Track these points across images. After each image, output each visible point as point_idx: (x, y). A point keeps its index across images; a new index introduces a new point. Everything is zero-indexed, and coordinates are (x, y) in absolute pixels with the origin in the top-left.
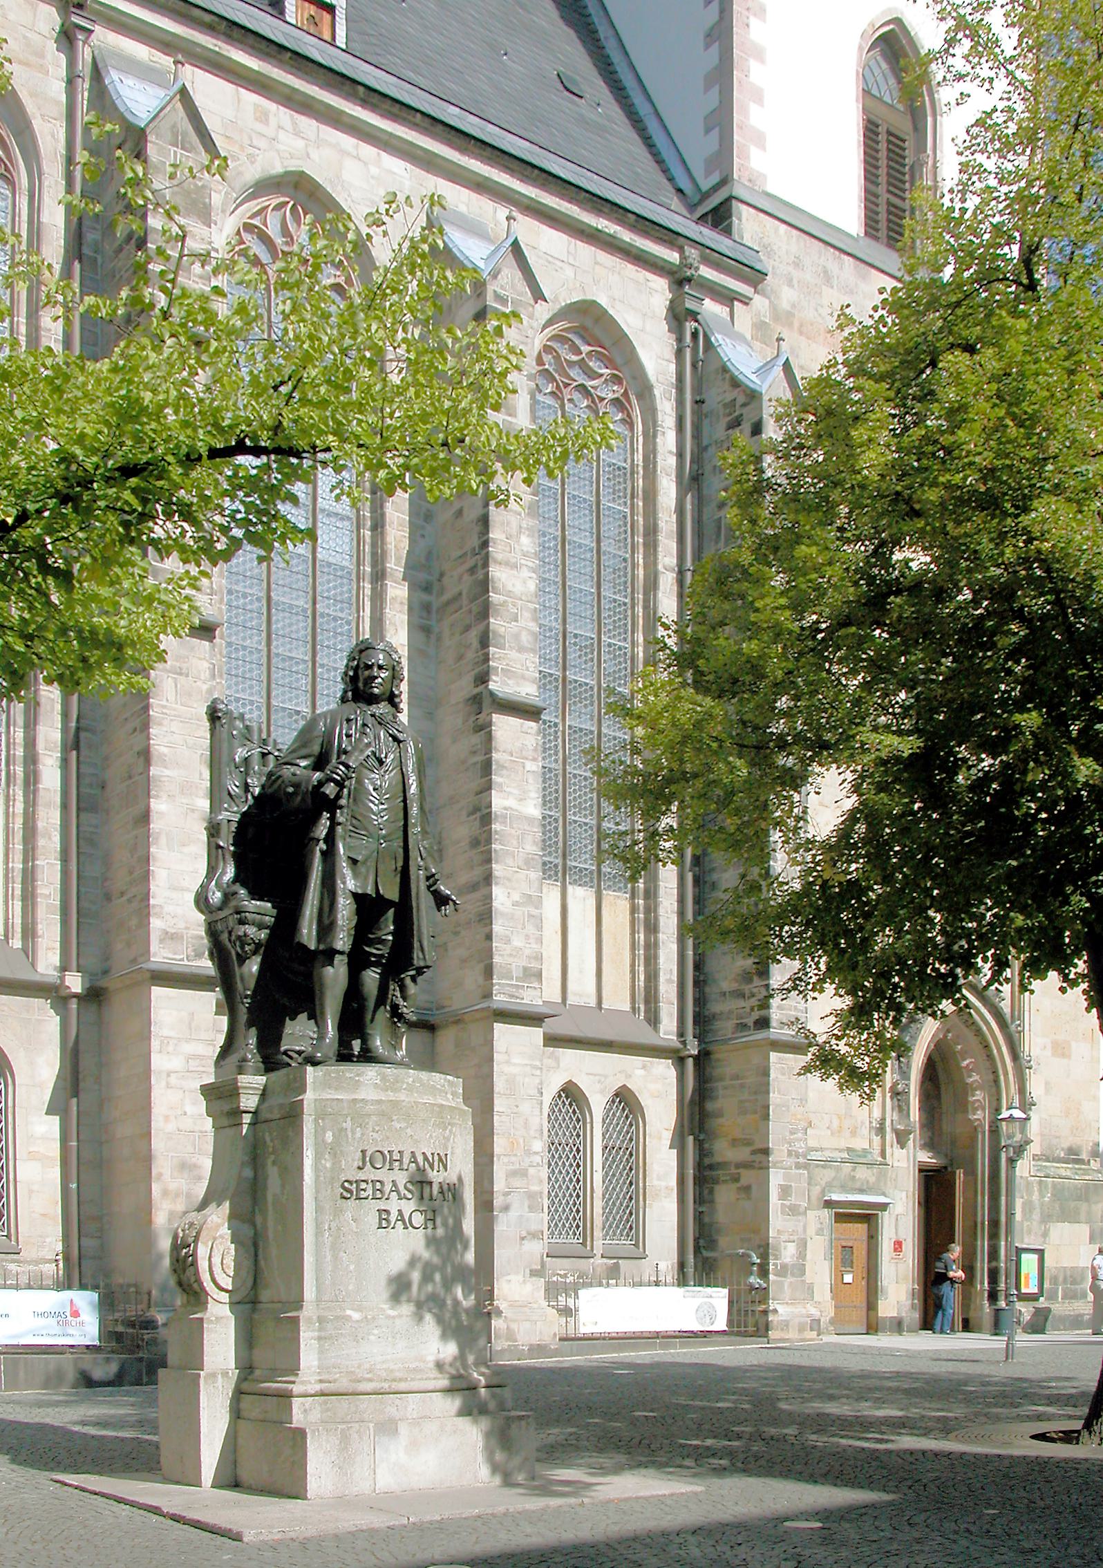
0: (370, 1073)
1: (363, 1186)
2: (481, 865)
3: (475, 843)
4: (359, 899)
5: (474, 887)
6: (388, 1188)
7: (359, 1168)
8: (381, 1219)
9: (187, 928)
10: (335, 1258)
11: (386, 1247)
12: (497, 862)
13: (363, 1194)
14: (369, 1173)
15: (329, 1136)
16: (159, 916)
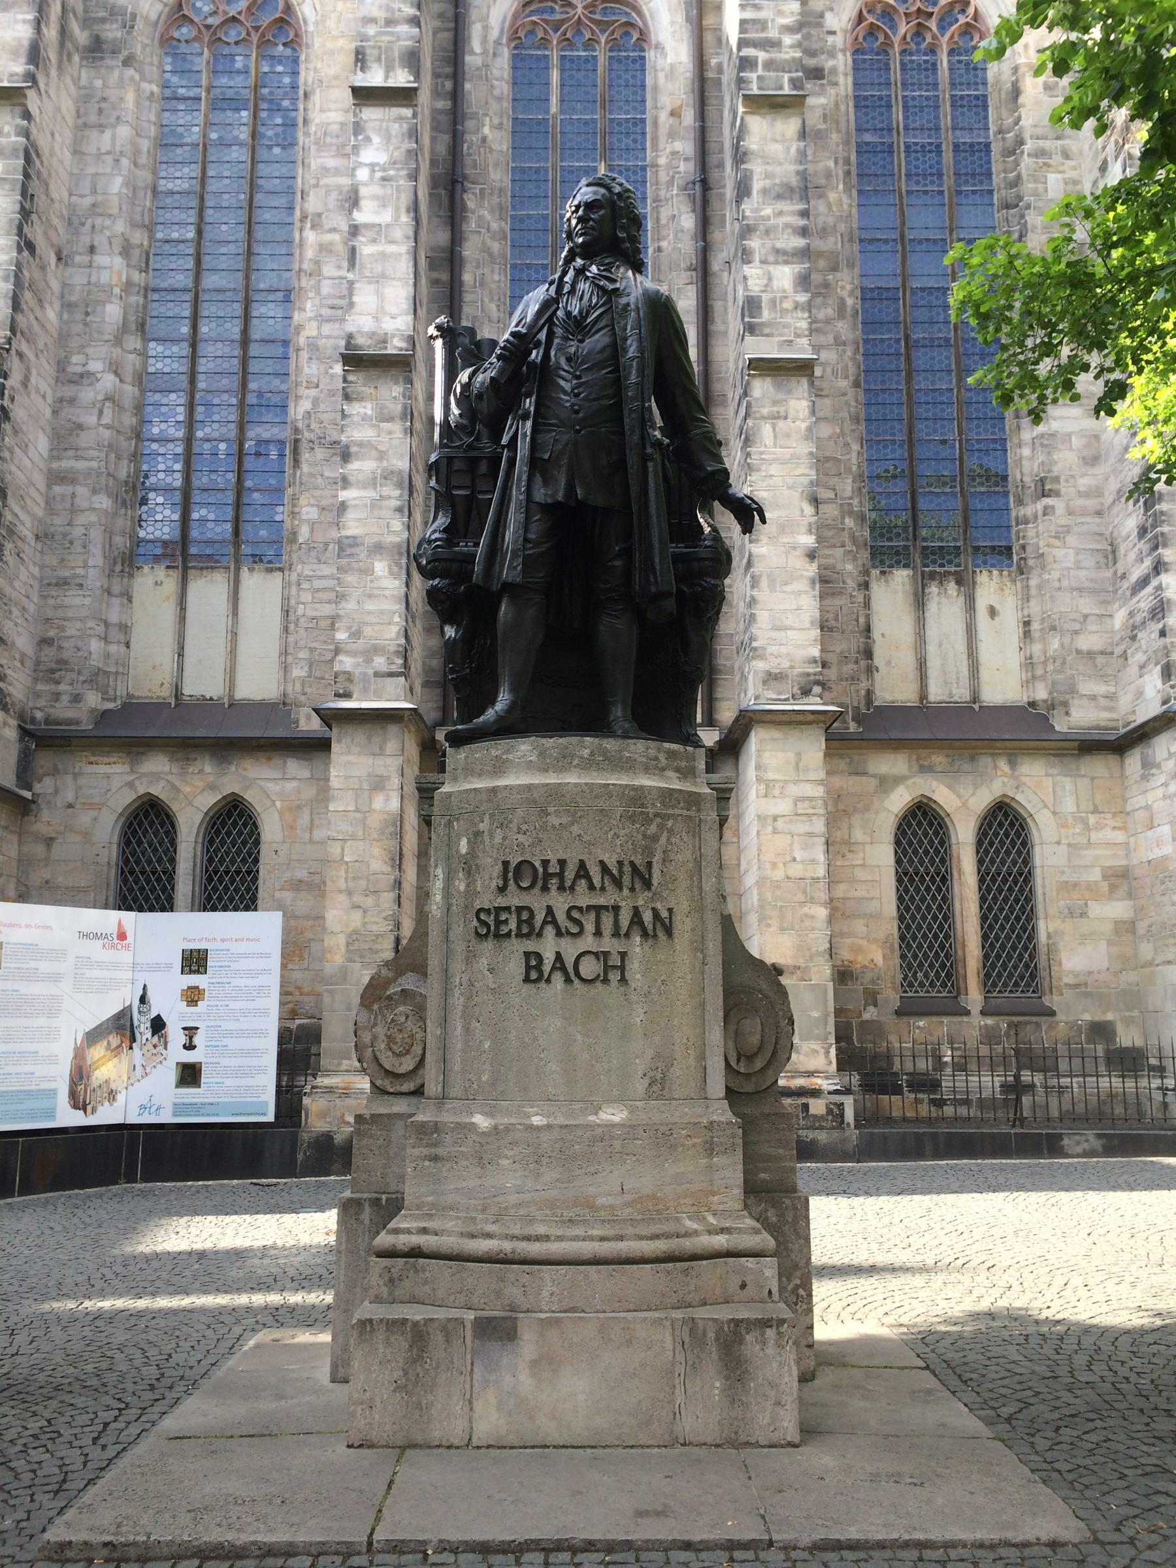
0: (524, 748)
1: (503, 917)
2: (1149, 555)
3: (1143, 531)
4: (549, 509)
5: (1144, 582)
6: (539, 917)
7: (502, 890)
8: (528, 968)
9: (792, 667)
10: (467, 1029)
11: (534, 1012)
12: (1165, 546)
13: (504, 930)
14: (514, 899)
15: (464, 846)
16: (762, 657)
